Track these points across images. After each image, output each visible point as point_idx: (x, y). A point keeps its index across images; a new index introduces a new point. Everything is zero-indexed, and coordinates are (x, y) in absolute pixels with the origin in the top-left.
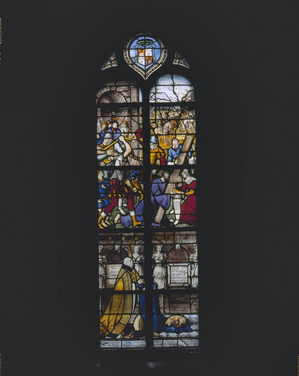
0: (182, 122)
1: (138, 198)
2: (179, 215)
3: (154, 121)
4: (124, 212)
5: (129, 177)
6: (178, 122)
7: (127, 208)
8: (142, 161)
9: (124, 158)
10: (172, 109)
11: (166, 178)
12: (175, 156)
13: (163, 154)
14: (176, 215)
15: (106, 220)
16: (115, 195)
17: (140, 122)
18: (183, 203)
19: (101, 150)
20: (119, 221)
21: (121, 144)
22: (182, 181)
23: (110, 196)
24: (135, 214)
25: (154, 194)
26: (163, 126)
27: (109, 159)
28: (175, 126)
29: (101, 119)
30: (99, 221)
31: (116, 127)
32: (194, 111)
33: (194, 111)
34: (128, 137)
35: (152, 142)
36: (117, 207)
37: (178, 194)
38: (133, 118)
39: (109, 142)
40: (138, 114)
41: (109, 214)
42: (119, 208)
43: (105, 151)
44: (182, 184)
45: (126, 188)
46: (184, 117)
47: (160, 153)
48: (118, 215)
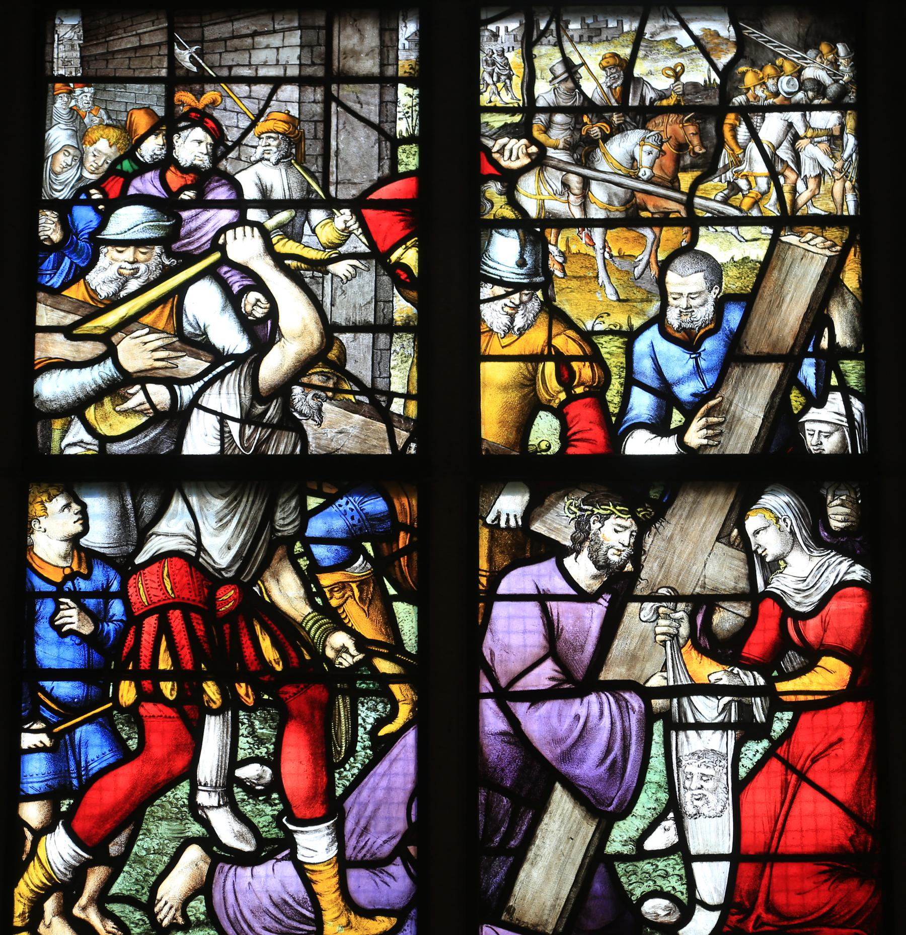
0: (743, 132)
1: (367, 716)
2: (725, 866)
3: (517, 118)
4: (238, 827)
5: (298, 547)
6: (711, 127)
7: (268, 801)
8: (407, 419)
9: (257, 396)
10: (664, 36)
11: (614, 559)
12: (686, 391)
13: (584, 371)
14: (697, 866)
15: (83, 900)
16: (167, 688)
17: (403, 127)
18: (759, 766)
19: (69, 332)
20: (198, 907)
21: (236, 288)
22: (743, 585)
23: (127, 693)
24: (334, 851)
25: (503, 682)
26: (586, 161)
27: (130, 404)
28: (688, 160)
29: (84, 96)
30: (20, 907)
31: (204, 162)
32: (841, 48)
33: (841, 48)
34: (297, 238)
35: (494, 273)
36: (184, 789)
37: (711, 690)
38: (347, 93)
39: (143, 267)
40: (383, 65)
41: (114, 849)
42: (202, 798)
43: (106, 337)
44: (744, 610)
45: (266, 629)
46: (759, 92)
47: (563, 362)
48: (194, 853)
